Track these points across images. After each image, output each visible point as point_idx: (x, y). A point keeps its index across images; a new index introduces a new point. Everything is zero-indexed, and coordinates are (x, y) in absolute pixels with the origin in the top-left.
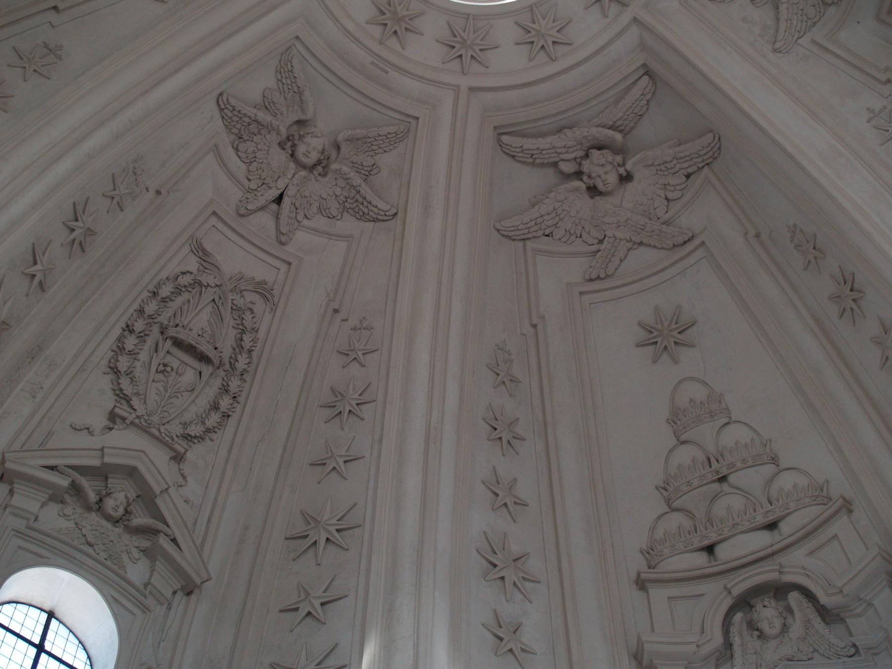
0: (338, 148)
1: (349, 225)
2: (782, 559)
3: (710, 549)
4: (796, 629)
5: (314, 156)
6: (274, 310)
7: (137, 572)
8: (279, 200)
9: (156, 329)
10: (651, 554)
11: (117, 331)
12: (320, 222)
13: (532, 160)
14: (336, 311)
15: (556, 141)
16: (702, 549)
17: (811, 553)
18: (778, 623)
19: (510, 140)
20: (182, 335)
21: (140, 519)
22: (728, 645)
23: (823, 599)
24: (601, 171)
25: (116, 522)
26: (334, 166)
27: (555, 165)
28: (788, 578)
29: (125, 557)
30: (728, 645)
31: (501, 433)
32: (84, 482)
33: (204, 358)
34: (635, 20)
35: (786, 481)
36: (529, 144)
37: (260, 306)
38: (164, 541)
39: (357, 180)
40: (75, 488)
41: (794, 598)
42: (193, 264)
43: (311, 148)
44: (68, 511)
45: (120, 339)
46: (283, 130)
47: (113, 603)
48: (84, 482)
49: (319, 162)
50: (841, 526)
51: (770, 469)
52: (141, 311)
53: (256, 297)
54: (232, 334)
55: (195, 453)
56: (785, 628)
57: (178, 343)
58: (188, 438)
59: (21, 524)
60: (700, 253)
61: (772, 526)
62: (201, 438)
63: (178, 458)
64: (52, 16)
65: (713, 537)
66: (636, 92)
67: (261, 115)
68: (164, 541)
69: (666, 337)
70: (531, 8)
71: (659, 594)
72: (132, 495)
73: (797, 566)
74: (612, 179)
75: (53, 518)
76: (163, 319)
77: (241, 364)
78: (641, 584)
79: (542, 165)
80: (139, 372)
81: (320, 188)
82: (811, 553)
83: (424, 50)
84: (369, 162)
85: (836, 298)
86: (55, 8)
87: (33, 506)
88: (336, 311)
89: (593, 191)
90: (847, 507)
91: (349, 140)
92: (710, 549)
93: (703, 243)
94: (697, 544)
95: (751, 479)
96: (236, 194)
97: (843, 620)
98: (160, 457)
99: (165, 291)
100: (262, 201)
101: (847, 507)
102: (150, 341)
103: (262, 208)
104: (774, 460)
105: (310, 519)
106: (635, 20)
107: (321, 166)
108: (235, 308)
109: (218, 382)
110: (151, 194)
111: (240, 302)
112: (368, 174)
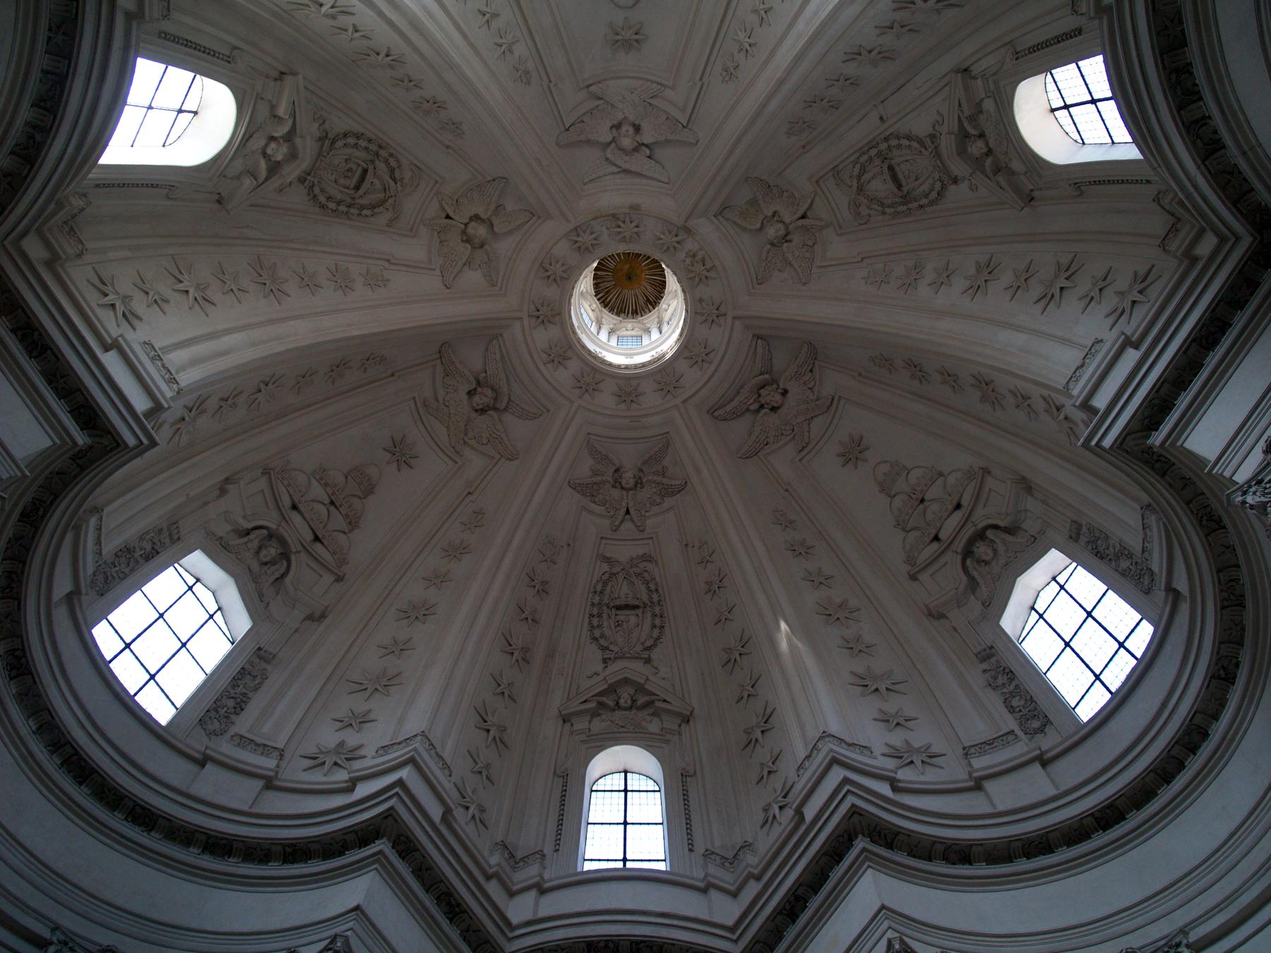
1: (669, 502)
2: (973, 519)
3: (936, 538)
4: (1001, 549)
5: (632, 482)
6: (657, 564)
7: (654, 726)
8: (628, 512)
9: (605, 608)
10: (910, 561)
11: (587, 620)
12: (655, 509)
13: (735, 415)
16: (932, 541)
18: (990, 551)
19: (718, 413)
20: (618, 602)
21: (642, 700)
22: (972, 579)
23: (1001, 524)
25: (630, 708)
27: (748, 409)
28: (980, 526)
29: (644, 723)
30: (972, 579)
31: (801, 550)
32: (604, 699)
33: (636, 607)
34: (734, 318)
35: (951, 480)
36: (728, 408)
37: (649, 566)
38: (659, 704)
39: (659, 479)
40: (601, 704)
41: (989, 533)
42: (606, 567)
43: (628, 478)
44: (604, 717)
45: (590, 623)
46: (610, 479)
47: (647, 747)
48: (604, 699)
49: (636, 483)
50: (990, 482)
51: (941, 480)
52: (593, 604)
53: (644, 564)
54: (643, 588)
55: (655, 654)
56: (995, 551)
57: (618, 608)
58: (648, 649)
59: (583, 737)
61: (958, 506)
62: (654, 645)
63: (648, 661)
64: (470, 498)
65: (934, 532)
66: (760, 350)
67: (594, 479)
68: (659, 704)
69: (853, 453)
71: (924, 577)
72: (632, 691)
73: (982, 517)
74: (778, 397)
75: (597, 725)
76: (606, 601)
77: (655, 597)
78: (913, 578)
79: (742, 414)
80: (607, 632)
81: (644, 494)
83: (651, 399)
85: (913, 377)
87: (585, 725)
89: (774, 409)
91: (644, 463)
92: (936, 538)
94: (928, 540)
95: (935, 492)
98: (638, 666)
99: (599, 588)
100: (620, 518)
101: (986, 471)
102: (605, 616)
104: (941, 474)
105: (728, 650)
106: (734, 318)
107: (639, 484)
108: (637, 575)
109: (649, 614)
111: (638, 571)
112: (663, 473)
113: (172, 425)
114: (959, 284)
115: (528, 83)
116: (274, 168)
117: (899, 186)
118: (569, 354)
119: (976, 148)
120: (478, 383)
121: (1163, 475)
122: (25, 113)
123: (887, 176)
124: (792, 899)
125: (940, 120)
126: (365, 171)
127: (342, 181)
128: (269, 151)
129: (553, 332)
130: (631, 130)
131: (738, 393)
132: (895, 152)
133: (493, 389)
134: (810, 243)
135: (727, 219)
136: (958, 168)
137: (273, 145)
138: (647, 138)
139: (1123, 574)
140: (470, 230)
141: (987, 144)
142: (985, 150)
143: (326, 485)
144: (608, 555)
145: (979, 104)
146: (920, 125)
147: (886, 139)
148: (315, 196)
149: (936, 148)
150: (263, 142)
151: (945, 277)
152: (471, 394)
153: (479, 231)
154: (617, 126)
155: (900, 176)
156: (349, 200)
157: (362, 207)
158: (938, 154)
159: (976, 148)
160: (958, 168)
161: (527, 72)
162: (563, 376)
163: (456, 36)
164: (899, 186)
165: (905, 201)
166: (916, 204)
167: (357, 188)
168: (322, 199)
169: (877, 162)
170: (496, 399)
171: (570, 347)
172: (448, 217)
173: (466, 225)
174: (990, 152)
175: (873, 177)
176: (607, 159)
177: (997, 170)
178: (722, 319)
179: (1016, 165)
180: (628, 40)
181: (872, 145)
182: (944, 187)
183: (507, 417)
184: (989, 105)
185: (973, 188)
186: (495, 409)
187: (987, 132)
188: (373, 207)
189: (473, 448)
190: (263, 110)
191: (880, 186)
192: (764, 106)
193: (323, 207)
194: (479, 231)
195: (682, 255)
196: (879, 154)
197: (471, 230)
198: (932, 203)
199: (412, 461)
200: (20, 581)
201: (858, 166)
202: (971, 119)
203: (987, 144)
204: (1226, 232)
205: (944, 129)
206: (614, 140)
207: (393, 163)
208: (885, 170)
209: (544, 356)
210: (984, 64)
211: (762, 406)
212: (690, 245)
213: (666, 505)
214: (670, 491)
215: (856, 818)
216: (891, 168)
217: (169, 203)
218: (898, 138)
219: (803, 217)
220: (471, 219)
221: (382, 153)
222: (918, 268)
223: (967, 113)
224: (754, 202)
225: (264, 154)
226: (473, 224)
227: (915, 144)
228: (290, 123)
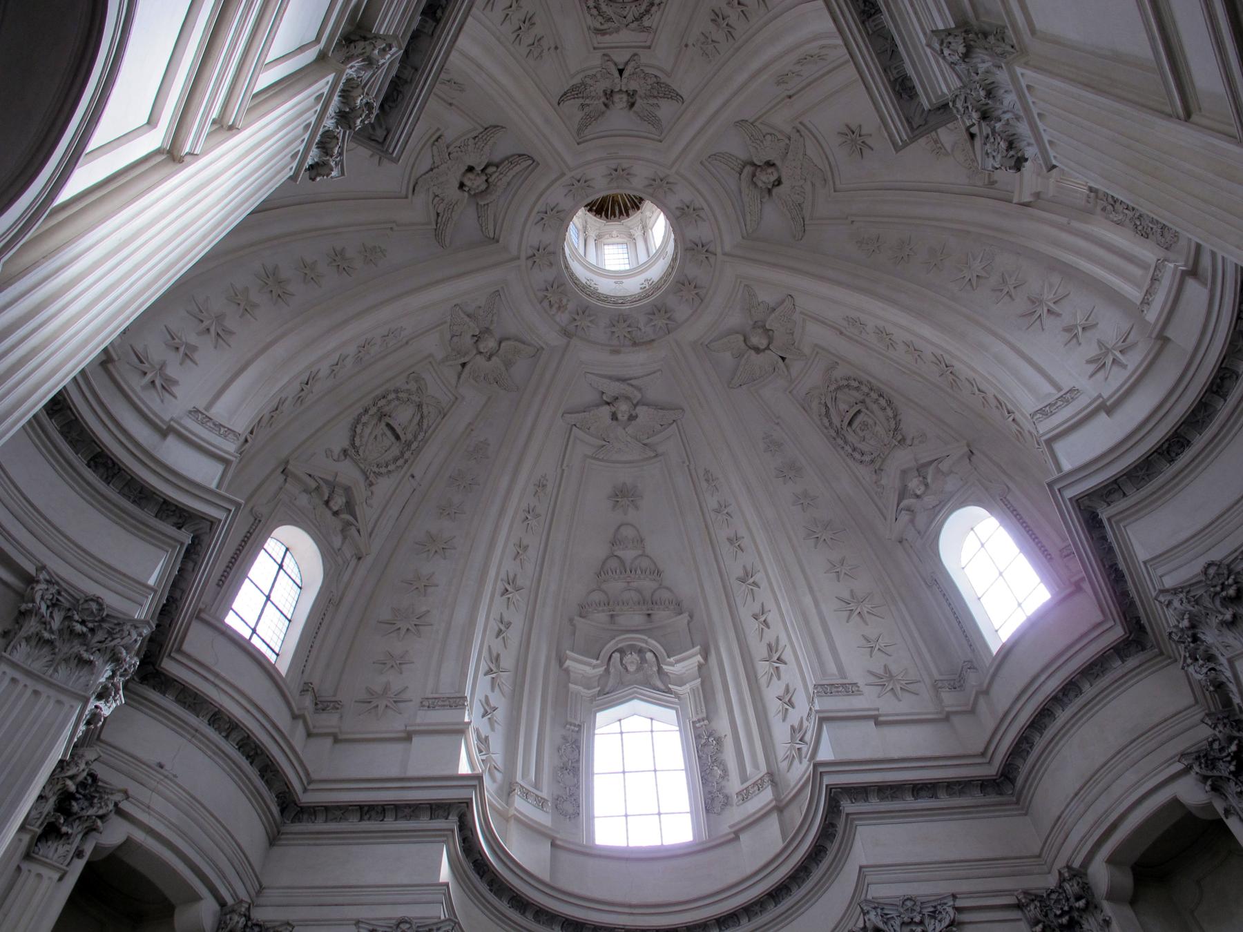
0: (606, 105)
5: (616, 98)
6: (589, 28)
8: (621, 72)
14: (556, 48)
15: (506, 179)
24: (476, 183)
26: (603, 99)
34: (518, 258)
36: (518, 168)
39: (588, 101)
42: (646, 24)
43: (620, 101)
60: (404, 192)
64: (791, 93)
66: (491, 227)
67: (655, 101)
70: (562, 220)
74: (467, 183)
79: (502, 162)
81: (604, 85)
84: (586, 109)
86: (790, 97)
88: (556, 48)
89: (471, 169)
93: (406, 197)
96: (645, 57)
99: (654, 9)
103: (627, 63)
106: (518, 258)
107: (609, 94)
108: (610, 20)
110: (690, 44)
111: (610, 24)
113: (1059, 315)
115: (707, 472)
116: (921, 470)
117: (388, 425)
118: (678, 213)
119: (338, 502)
120: (770, 191)
121: (165, 502)
122: (1062, 716)
123: (399, 431)
124: (439, 13)
126: (850, 424)
127: (870, 422)
128: (923, 488)
129: (692, 233)
130: (619, 416)
131: (509, 184)
132: (397, 453)
133: (755, 185)
134: (455, 339)
135: (529, 345)
137: (919, 493)
138: (606, 411)
140: (765, 342)
141: (330, 509)
142: (332, 504)
143: (936, 142)
144: (645, 34)
145: (345, 538)
146: (384, 486)
147: (406, 461)
148: (895, 416)
149: (367, 478)
150: (926, 499)
152: (779, 182)
153: (758, 340)
154: (632, 418)
155: (389, 433)
156: (868, 400)
157: (857, 389)
158: (364, 473)
159: (338, 502)
160: (348, 472)
161: (707, 480)
162: (683, 194)
163: (761, 548)
164: (388, 425)
166: (371, 412)
167: (859, 412)
168: (888, 409)
169: (410, 437)
170: (754, 175)
171: (677, 218)
172: (783, 359)
173: (768, 348)
174: (327, 503)
175: (411, 421)
176: (640, 390)
177: (318, 488)
178: (530, 252)
179: (303, 500)
180: (624, 496)
181: (419, 450)
182: (353, 445)
183: (743, 156)
184: (337, 541)
186: (753, 164)
188: (848, 386)
189: (780, 132)
190: (921, 520)
191: (403, 416)
192: (513, 481)
193: (889, 402)
194: (758, 340)
195: (571, 306)
197: (763, 340)
198: (358, 420)
199: (846, 130)
200: (1212, 384)
201: (425, 427)
202: (352, 524)
203: (330, 509)
204: (178, 657)
206: (635, 406)
207: (826, 421)
208: (402, 436)
209: (702, 214)
211: (483, 170)
212: (563, 318)
213: (581, 76)
214: (575, 92)
215: (380, 133)
216: (398, 438)
217: (1011, 485)
219: (464, 365)
220: (764, 350)
221: (834, 434)
222: (358, 360)
223: (353, 531)
224: (508, 364)
225: (927, 485)
226: (762, 347)
227: (383, 470)
228: (902, 505)
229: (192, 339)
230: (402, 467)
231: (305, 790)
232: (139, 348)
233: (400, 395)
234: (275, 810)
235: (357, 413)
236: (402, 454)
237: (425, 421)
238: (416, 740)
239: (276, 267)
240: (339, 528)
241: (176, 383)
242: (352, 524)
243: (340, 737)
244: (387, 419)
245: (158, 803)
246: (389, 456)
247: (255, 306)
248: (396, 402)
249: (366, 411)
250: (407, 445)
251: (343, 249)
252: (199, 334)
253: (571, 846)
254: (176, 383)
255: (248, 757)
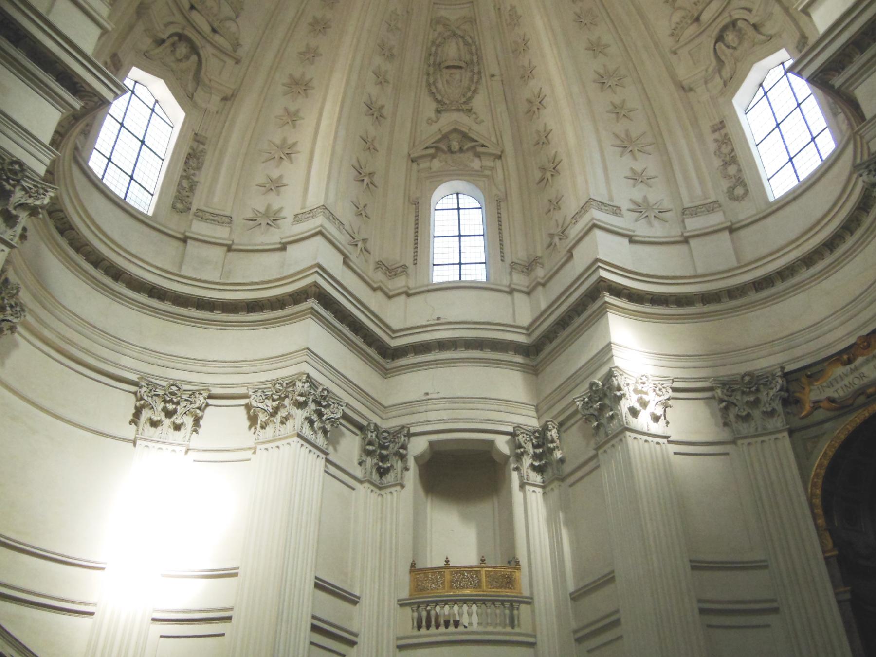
3: (192, 7)
4: (184, 65)
17: (213, 55)
35: (233, 27)
41: (194, 58)
50: (230, 62)
51: (233, 15)
56: (180, 60)
61: (214, 31)
65: (199, 7)
82: (213, 55)
90: (238, 62)
92: (192, 7)
97: (198, 84)
101: (238, 62)
104: (237, 17)
114: (374, 90)
117: (448, 67)
119: (455, 145)
123: (456, 64)
125: (478, 120)
132: (469, 74)
136: (448, 120)
139: (180, 184)
145: (479, 157)
146: (479, 103)
147: (479, 73)
149: (463, 110)
151: (381, 79)
158: (458, 110)
164: (448, 67)
165: (436, 66)
166: (431, 72)
169: (468, 58)
175: (459, 49)
177: (437, 149)
179: (436, 164)
181: (480, 58)
182: (438, 101)
184: (476, 164)
185: (430, 122)
187: (462, 155)
191: (452, 51)
196: (472, 61)
198: (429, 85)
201: (470, 41)
205: (475, 126)
210: (500, 171)
216: (460, 67)
218: (477, 83)
222: (391, 57)
227: (469, 94)
229: (275, 174)
230: (481, 78)
231: (529, 335)
232: (250, 215)
233: (438, 42)
234: (519, 359)
235: (424, 83)
236: (472, 71)
237: (468, 38)
238: (575, 252)
239: (291, 76)
240: (470, 154)
241: (281, 210)
242: (473, 147)
243: (542, 281)
244: (443, 66)
245: (433, 416)
246: (466, 83)
247: (298, 111)
248: (440, 49)
249: (428, 74)
250: (471, 65)
251: (314, 17)
252: (278, 167)
253: (743, 223)
254: (281, 210)
255: (477, 349)
